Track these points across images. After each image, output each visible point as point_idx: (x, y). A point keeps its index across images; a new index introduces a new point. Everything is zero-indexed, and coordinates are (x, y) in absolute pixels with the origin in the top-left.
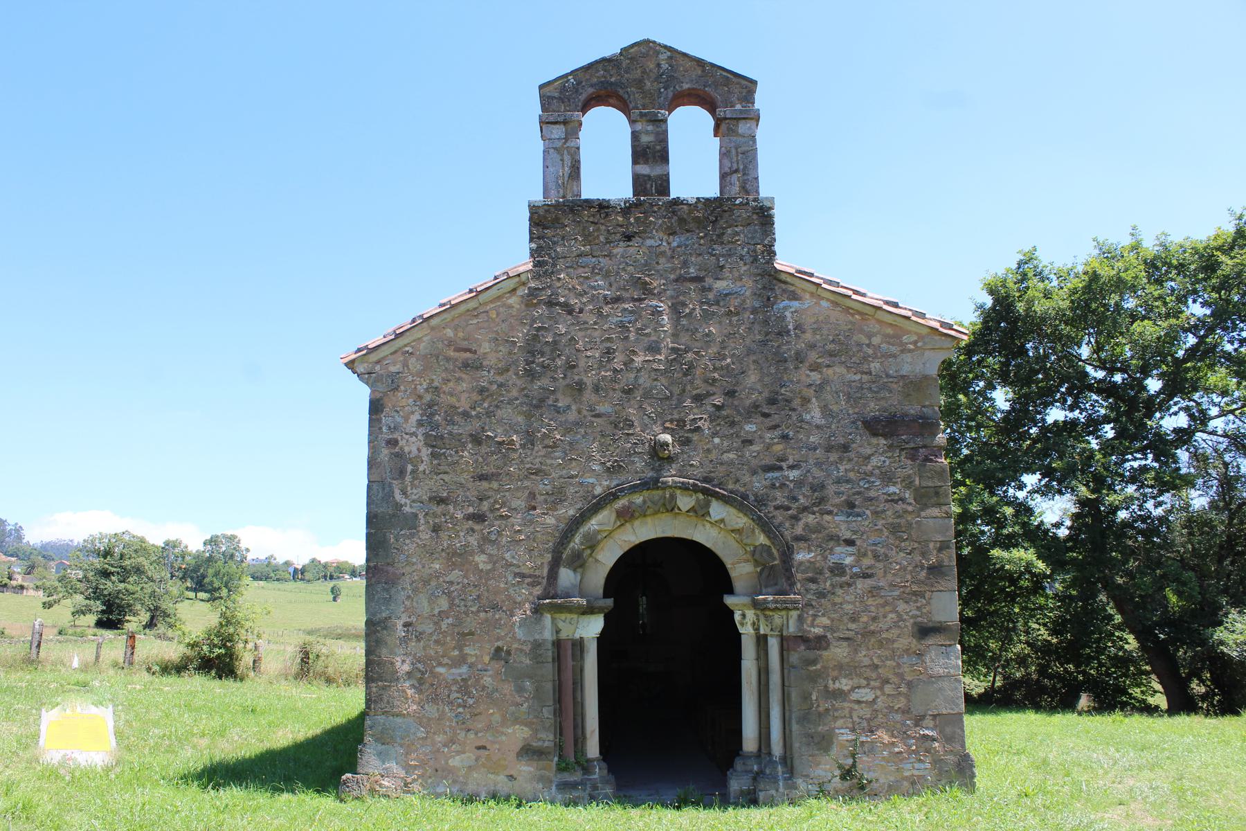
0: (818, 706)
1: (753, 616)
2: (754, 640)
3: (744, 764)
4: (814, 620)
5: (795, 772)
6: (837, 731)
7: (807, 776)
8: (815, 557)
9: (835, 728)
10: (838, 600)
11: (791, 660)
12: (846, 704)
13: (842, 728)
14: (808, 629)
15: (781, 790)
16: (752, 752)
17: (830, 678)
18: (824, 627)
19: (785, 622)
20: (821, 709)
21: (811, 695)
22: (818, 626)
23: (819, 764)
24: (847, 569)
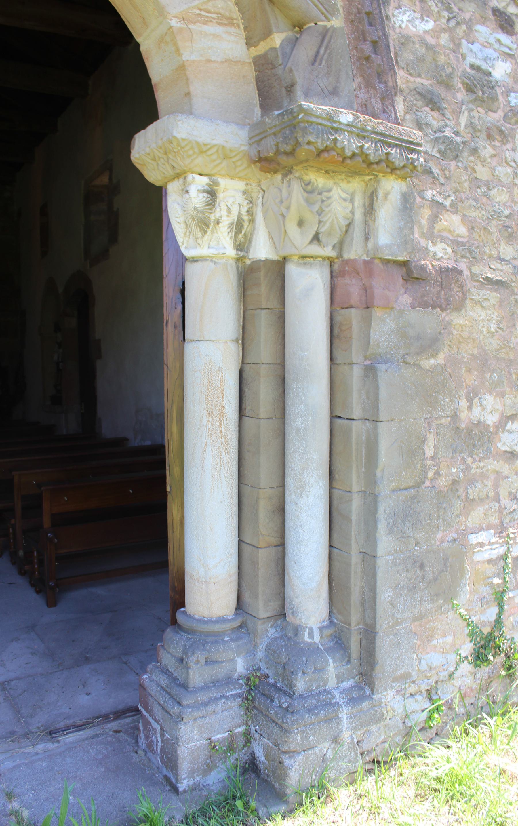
0: (437, 474)
1: (240, 198)
2: (232, 278)
3: (208, 662)
4: (434, 218)
5: (378, 673)
6: (473, 539)
7: (406, 677)
8: (436, 32)
9: (465, 533)
10: (483, 173)
11: (374, 335)
12: (492, 465)
13: (481, 529)
14: (423, 243)
15: (346, 736)
16: (222, 620)
17: (462, 393)
18: (456, 243)
19: (359, 216)
20: (442, 482)
21: (424, 441)
22: (443, 239)
23: (430, 637)
24: (499, 91)
